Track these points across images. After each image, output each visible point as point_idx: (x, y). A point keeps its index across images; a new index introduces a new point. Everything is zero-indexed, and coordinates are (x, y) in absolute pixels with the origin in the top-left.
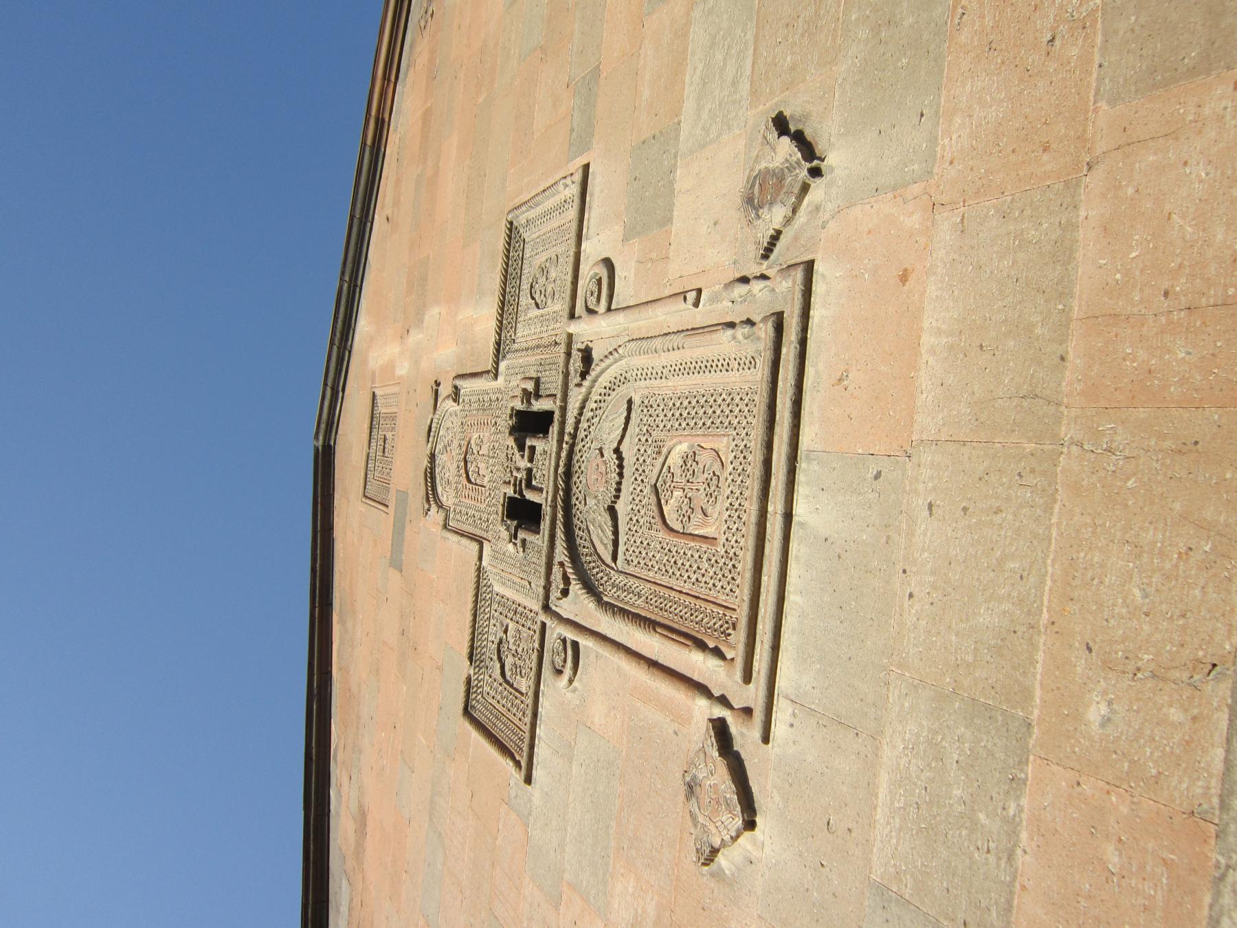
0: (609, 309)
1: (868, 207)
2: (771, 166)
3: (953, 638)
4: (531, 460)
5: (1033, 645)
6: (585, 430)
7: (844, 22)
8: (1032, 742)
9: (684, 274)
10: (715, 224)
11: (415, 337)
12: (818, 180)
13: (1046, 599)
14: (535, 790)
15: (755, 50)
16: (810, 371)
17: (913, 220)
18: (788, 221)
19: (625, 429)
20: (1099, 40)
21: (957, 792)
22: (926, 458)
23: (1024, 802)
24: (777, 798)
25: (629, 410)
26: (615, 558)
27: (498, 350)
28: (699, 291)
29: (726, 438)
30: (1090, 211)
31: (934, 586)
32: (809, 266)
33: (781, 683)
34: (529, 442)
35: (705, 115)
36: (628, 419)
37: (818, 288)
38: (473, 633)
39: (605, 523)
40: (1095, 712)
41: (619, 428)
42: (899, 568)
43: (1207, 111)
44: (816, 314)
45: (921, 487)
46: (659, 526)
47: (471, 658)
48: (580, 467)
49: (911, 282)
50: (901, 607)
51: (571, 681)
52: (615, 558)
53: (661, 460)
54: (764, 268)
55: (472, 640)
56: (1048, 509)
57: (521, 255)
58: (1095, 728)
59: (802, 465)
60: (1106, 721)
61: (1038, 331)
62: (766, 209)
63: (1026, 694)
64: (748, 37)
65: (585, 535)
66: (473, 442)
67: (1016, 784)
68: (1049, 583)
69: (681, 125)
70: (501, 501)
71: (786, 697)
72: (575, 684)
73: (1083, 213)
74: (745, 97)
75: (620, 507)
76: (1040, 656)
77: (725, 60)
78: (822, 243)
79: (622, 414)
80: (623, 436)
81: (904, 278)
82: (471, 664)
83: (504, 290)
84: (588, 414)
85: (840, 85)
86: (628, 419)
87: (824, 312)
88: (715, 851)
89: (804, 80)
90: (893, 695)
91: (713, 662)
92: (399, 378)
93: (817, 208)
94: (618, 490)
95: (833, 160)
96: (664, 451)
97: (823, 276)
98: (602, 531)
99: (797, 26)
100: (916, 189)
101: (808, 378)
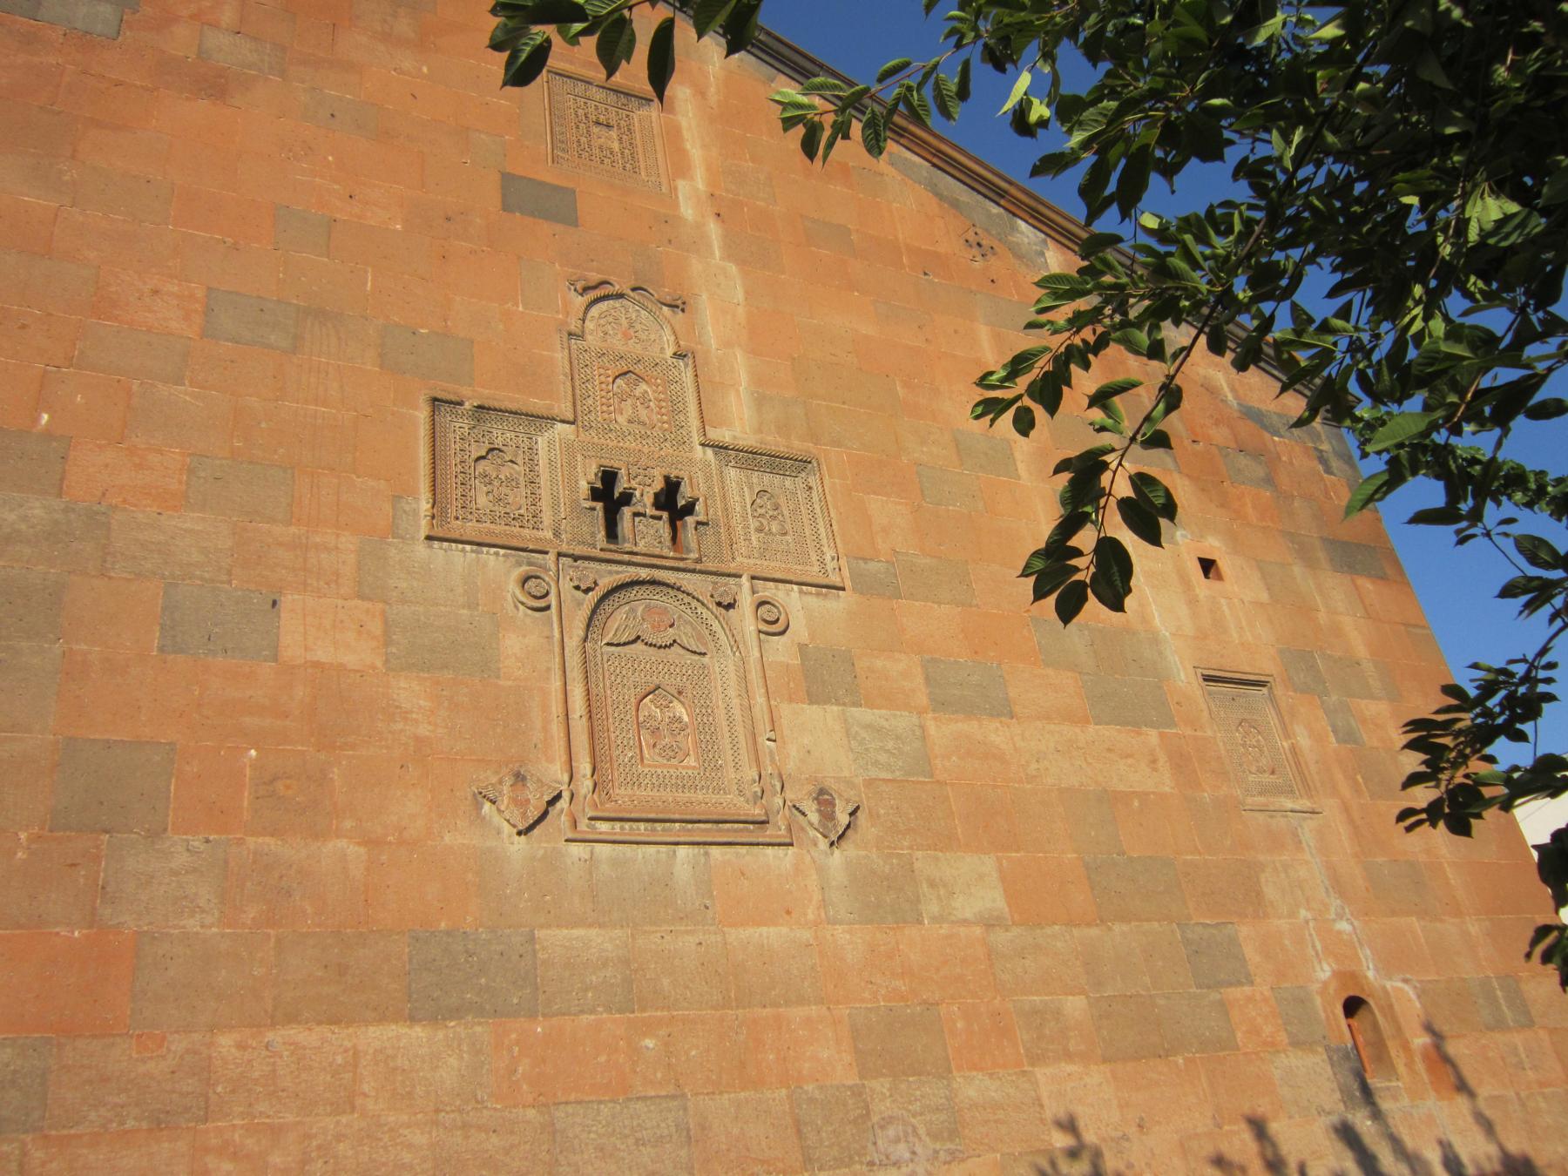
0: (760, 632)
2: (837, 809)
3: (653, 966)
4: (653, 517)
5: (663, 1009)
8: (628, 1014)
11: (713, 229)
12: (828, 845)
13: (680, 1012)
14: (421, 550)
15: (889, 780)
16: (743, 850)
17: (811, 917)
18: (811, 824)
19: (688, 650)
20: (869, 1006)
21: (594, 978)
22: (719, 938)
23: (605, 1015)
24: (541, 852)
25: (700, 654)
26: (608, 644)
27: (721, 447)
28: (775, 741)
30: (813, 1010)
31: (670, 951)
32: (791, 844)
33: (598, 847)
34: (665, 515)
36: (695, 652)
37: (781, 851)
38: (501, 411)
40: (649, 1043)
42: (673, 928)
43: (844, 1054)
44: (769, 850)
45: (707, 936)
46: (639, 697)
47: (480, 407)
49: (787, 917)
50: (656, 932)
51: (522, 603)
52: (608, 644)
53: (676, 695)
54: (788, 803)
55: (495, 410)
56: (713, 1008)
57: (787, 473)
58: (643, 1044)
59: (702, 849)
60: (647, 1048)
61: (773, 993)
63: (643, 1010)
64: (898, 773)
65: (616, 604)
66: (644, 386)
67: (609, 1010)
68: (687, 1013)
70: (615, 465)
71: (592, 853)
72: (521, 607)
73: (814, 1007)
75: (639, 646)
76: (659, 1013)
77: (888, 751)
80: (684, 648)
81: (788, 913)
83: (764, 455)
84: (694, 603)
86: (695, 652)
88: (494, 803)
89: (872, 826)
90: (618, 932)
91: (589, 784)
92: (676, 189)
93: (816, 845)
94: (651, 645)
95: (837, 852)
96: (681, 698)
97: (786, 855)
100: (823, 915)
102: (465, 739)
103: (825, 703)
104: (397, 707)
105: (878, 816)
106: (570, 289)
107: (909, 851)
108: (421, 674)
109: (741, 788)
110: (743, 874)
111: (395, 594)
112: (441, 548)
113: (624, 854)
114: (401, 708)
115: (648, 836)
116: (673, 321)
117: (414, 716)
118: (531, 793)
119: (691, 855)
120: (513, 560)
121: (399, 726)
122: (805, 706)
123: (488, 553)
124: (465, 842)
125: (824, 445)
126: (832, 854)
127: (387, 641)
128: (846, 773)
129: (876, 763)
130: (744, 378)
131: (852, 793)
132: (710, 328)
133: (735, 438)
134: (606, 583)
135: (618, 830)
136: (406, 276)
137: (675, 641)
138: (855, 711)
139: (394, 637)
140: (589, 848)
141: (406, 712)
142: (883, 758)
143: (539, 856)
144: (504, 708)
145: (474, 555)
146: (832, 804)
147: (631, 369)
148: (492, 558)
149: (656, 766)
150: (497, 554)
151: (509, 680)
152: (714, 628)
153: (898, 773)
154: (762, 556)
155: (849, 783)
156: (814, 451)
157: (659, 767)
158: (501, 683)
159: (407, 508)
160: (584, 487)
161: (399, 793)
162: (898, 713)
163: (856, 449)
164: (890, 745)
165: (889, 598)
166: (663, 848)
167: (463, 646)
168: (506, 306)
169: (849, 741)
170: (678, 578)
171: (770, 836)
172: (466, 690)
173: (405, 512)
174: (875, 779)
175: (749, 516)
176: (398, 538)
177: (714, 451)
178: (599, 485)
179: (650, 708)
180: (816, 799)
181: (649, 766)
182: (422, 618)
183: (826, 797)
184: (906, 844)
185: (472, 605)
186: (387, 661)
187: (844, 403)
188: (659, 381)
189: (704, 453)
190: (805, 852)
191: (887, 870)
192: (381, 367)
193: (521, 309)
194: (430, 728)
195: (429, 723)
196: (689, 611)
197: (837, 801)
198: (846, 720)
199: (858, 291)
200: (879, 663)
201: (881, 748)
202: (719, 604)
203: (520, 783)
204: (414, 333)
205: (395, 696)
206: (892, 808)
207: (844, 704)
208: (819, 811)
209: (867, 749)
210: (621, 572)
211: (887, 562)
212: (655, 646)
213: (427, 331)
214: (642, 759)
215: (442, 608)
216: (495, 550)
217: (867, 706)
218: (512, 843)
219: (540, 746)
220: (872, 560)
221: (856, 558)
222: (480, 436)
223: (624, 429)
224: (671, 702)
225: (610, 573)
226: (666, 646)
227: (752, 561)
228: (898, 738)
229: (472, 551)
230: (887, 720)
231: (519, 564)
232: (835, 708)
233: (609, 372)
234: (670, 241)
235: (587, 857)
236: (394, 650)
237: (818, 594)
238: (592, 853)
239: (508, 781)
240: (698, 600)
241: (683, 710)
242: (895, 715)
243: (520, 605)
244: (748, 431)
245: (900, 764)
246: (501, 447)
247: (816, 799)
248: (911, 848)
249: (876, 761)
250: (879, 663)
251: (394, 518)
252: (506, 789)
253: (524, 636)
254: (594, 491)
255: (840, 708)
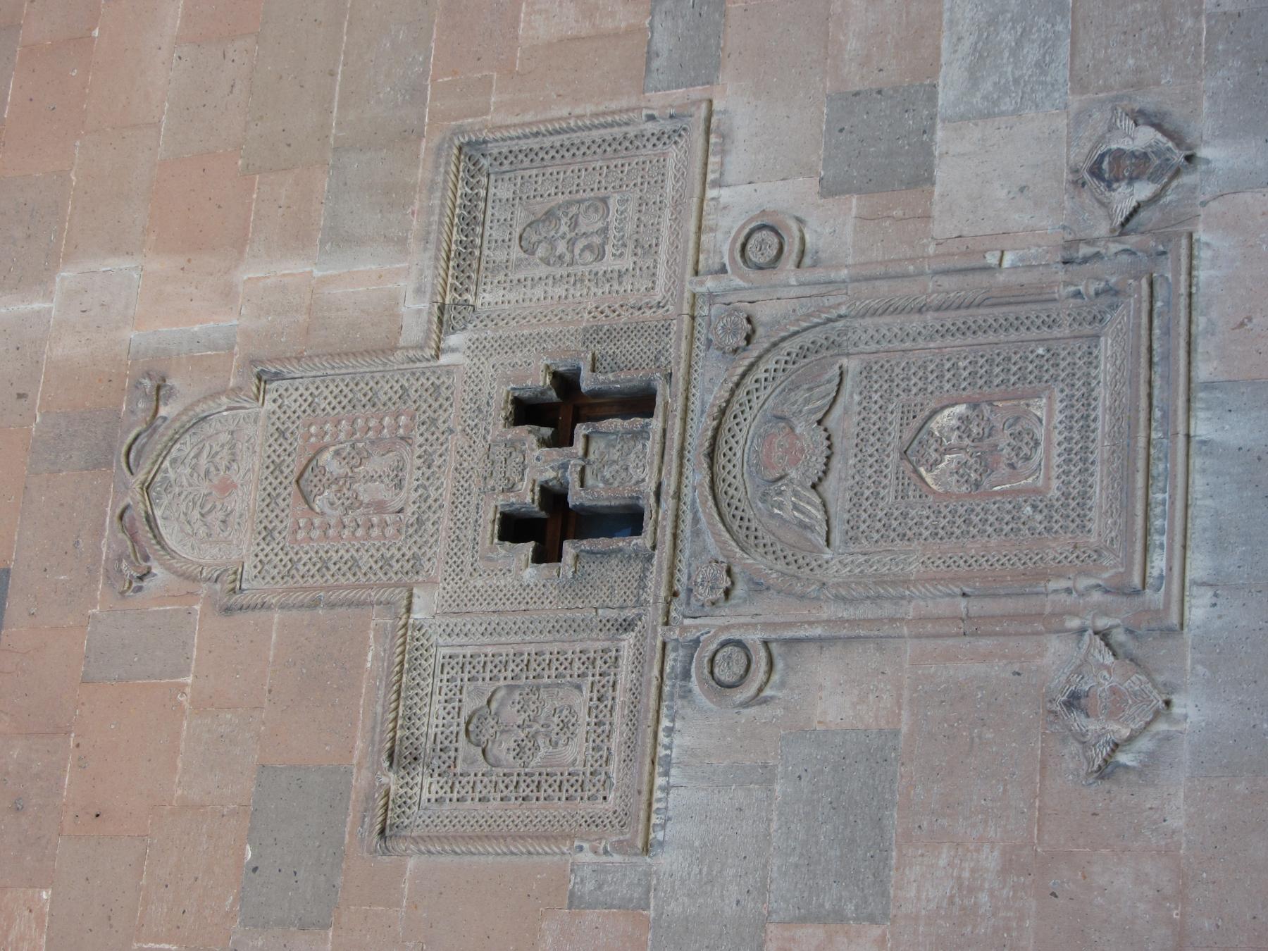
1: (1259, 195)
2: (1127, 148)
6: (741, 405)
7: (1207, 49)
9: (965, 233)
10: (1022, 189)
15: (1073, 43)
16: (1201, 322)
29: (1047, 392)
35: (987, 86)
39: (808, 503)
41: (824, 397)
44: (1202, 275)
48: (730, 449)
62: (1124, 184)
64: (1060, 28)
69: (940, 89)
71: (1203, 584)
72: (768, 692)
74: (1062, 81)
77: (1019, 43)
78: (1201, 218)
79: (829, 381)
82: (391, 765)
85: (1210, 97)
87: (1212, 272)
89: (1157, 83)
93: (1193, 189)
95: (1204, 152)
97: (1208, 245)
98: (803, 513)
99: (1140, 38)
101: (1198, 326)
102: (1005, 791)
103: (930, 154)
104: (952, 902)
105: (1138, 70)
106: (140, 589)
107: (1203, 18)
108: (893, 862)
109: (1089, 318)
110: (1242, 324)
111: (751, 905)
112: (663, 827)
113: (1205, 530)
114: (952, 897)
115: (1174, 487)
116: (189, 401)
117: (966, 874)
118: (1099, 684)
119: (1208, 414)
120: (679, 702)
121: (984, 898)
122: (937, 190)
123: (668, 747)
124: (1182, 795)
125: (422, 118)
126: (1208, 162)
127: (841, 918)
128: (1062, 123)
129: (1041, 66)
130: (294, 268)
131: (1097, 115)
132: (196, 328)
133: (419, 291)
134: (714, 539)
135: (1165, 538)
136: (143, 882)
137: (819, 422)
138: (945, 97)
139: (827, 906)
140: (1195, 588)
141: (960, 887)
142: (1032, 53)
143: (1208, 674)
144: (952, 726)
145: (673, 771)
146: (1118, 155)
147: (293, 478)
148: (677, 740)
149: (1048, 467)
150: (670, 731)
151: (900, 714)
152: (795, 350)
153: (1060, 28)
154: (652, 250)
155: (1079, 120)
156: (436, 140)
157: (1048, 459)
158: (904, 729)
159: (590, 885)
160: (531, 573)
161: (1100, 900)
162: (946, 16)
163: (427, 58)
164: (1007, 37)
165: (724, 15)
166: (1196, 462)
167: (842, 792)
168: (187, 705)
169: (1002, 114)
170: (703, 412)
171: (1177, 273)
172: (919, 789)
173: (600, 887)
174: (1072, 70)
175: (570, 269)
176: (648, 899)
177: (447, 333)
178: (528, 548)
179: (943, 472)
180: (1109, 186)
181: (1048, 478)
182: (792, 860)
183: (1105, 165)
184: (1190, 23)
185: (766, 777)
186: (872, 919)
187: (332, 74)
188: (313, 429)
189: (453, 350)
190: (1202, 212)
191: (1237, 64)
192: (326, 927)
193: (189, 680)
194: (986, 849)
195: (978, 850)
196: (763, 394)
197: (1114, 146)
198: (963, 117)
199: (91, 30)
200: (852, 44)
201: (1013, 53)
202: (748, 339)
203: (1083, 701)
204: (255, 869)
205: (933, 905)
206: (1125, 44)
207: (932, 118)
208: (1132, 180)
209: (1016, 81)
210: (695, 514)
211: (652, 14)
212: (828, 458)
213: (248, 847)
214: (1036, 491)
215: (774, 826)
216: (661, 735)
217: (935, 73)
218: (1186, 716)
219: (1016, 668)
220: (649, 43)
221: (648, 70)
222: (445, 756)
223: (414, 495)
224: (931, 434)
225: (697, 533)
226: (828, 438)
227: (662, 270)
228: (993, 21)
229: (666, 774)
230: (959, 39)
231: (686, 694)
232: (940, 134)
233: (302, 522)
234: (20, 396)
235: (1210, 593)
236: (851, 907)
237: (723, 153)
238: (1203, 584)
239: (1077, 721)
240: (743, 376)
241: (946, 412)
242: (951, 21)
243: (764, 694)
244: (406, 265)
245: (1042, 20)
246: (462, 721)
247: (1109, 186)
248: (1197, 15)
249: (1038, 65)
250: (853, 45)
251: (610, 908)
252: (1093, 726)
253: (821, 688)
254: (539, 558)
255: (939, 125)
